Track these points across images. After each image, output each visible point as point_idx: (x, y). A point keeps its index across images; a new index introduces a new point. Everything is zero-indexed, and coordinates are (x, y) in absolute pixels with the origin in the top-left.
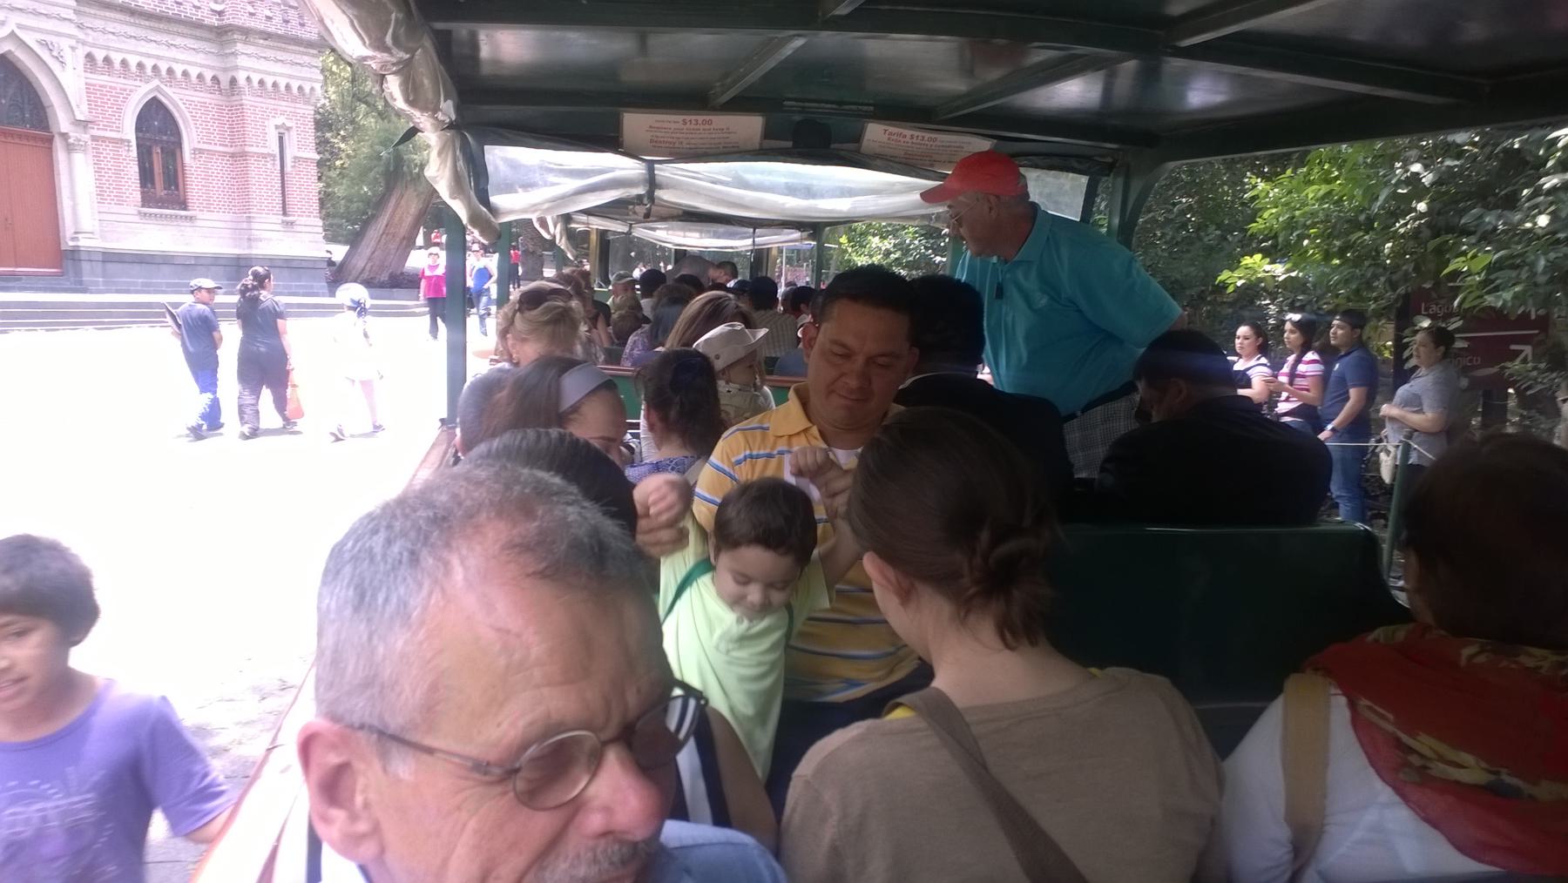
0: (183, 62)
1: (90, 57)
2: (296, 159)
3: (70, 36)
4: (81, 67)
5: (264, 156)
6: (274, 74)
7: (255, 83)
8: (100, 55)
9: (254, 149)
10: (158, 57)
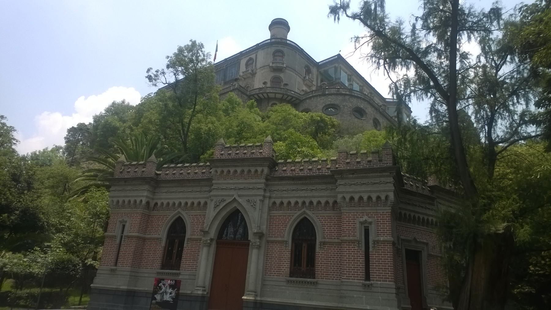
0: (318, 197)
1: (274, 203)
2: (376, 242)
3: (260, 195)
4: (266, 209)
5: (353, 242)
6: (359, 192)
7: (347, 200)
8: (278, 201)
9: (345, 238)
10: (305, 197)
